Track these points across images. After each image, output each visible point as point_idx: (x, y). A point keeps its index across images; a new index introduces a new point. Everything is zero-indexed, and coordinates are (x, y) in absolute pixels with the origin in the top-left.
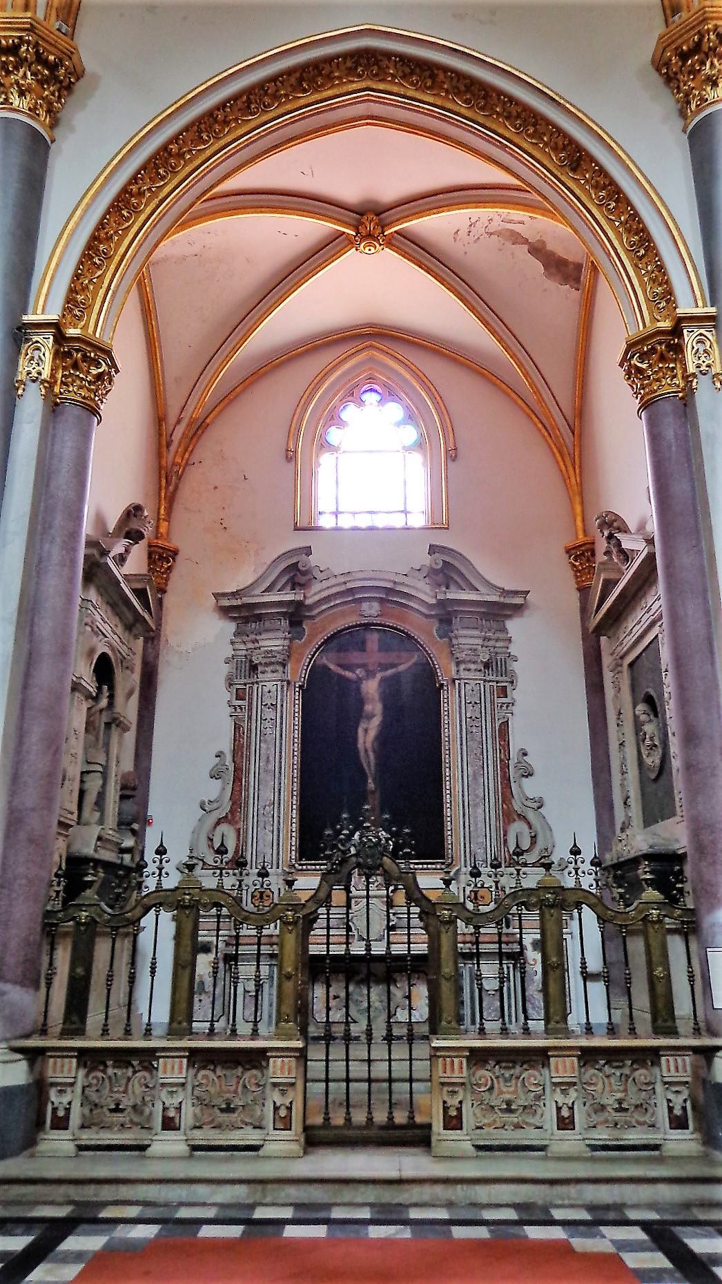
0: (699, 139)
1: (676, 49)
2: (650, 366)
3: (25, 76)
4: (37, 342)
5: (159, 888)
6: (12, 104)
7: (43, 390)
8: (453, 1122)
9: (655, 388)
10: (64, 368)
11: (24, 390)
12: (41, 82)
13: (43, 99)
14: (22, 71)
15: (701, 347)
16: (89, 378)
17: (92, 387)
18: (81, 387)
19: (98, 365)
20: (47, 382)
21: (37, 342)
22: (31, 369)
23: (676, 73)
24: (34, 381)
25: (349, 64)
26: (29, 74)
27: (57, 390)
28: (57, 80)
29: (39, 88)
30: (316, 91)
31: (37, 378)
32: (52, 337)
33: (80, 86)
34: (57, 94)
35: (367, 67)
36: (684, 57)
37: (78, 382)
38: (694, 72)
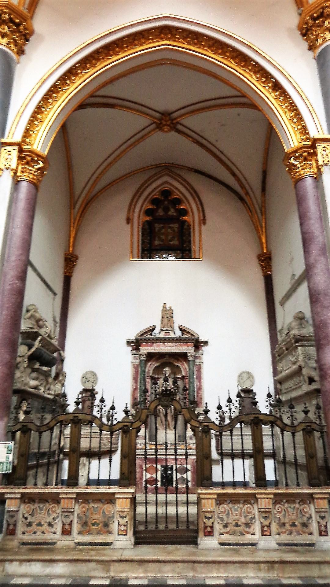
0: (321, 60)
1: (310, 16)
2: (300, 163)
4: (9, 151)
10: (22, 165)
12: (12, 32)
15: (324, 153)
16: (34, 170)
17: (35, 174)
18: (30, 173)
19: (38, 164)
20: (15, 170)
21: (9, 151)
23: (311, 27)
24: (7, 169)
25: (157, 33)
27: (19, 174)
30: (142, 45)
33: (32, 39)
35: (166, 34)
36: (315, 19)
38: (320, 26)
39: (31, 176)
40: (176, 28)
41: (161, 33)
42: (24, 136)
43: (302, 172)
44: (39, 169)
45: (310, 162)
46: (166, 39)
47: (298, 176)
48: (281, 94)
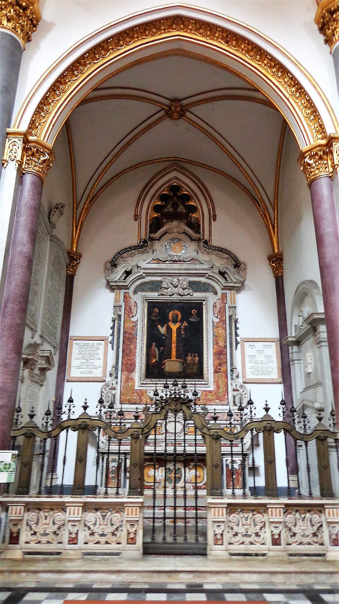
2: (315, 162)
3: (10, 11)
4: (15, 142)
5: (69, 419)
6: (3, 25)
7: (17, 165)
8: (218, 540)
9: (317, 173)
10: (27, 156)
11: (7, 165)
12: (19, 15)
13: (19, 23)
14: (8, 9)
17: (41, 166)
18: (36, 166)
20: (20, 162)
21: (15, 142)
22: (11, 155)
25: (169, 24)
26: (12, 10)
27: (23, 167)
28: (26, 16)
29: (17, 18)
30: (153, 35)
31: (14, 159)
32: (22, 140)
34: (26, 23)
35: (178, 25)
37: (33, 163)
39: (36, 168)
40: (189, 19)
41: (173, 23)
42: (29, 128)
43: (317, 172)
44: (44, 161)
45: (325, 162)
46: (178, 30)
47: (313, 175)
48: (297, 90)
